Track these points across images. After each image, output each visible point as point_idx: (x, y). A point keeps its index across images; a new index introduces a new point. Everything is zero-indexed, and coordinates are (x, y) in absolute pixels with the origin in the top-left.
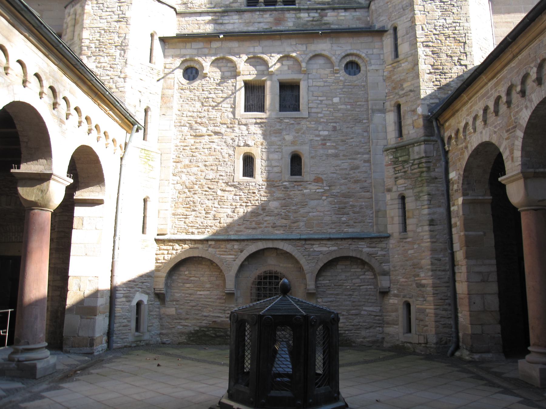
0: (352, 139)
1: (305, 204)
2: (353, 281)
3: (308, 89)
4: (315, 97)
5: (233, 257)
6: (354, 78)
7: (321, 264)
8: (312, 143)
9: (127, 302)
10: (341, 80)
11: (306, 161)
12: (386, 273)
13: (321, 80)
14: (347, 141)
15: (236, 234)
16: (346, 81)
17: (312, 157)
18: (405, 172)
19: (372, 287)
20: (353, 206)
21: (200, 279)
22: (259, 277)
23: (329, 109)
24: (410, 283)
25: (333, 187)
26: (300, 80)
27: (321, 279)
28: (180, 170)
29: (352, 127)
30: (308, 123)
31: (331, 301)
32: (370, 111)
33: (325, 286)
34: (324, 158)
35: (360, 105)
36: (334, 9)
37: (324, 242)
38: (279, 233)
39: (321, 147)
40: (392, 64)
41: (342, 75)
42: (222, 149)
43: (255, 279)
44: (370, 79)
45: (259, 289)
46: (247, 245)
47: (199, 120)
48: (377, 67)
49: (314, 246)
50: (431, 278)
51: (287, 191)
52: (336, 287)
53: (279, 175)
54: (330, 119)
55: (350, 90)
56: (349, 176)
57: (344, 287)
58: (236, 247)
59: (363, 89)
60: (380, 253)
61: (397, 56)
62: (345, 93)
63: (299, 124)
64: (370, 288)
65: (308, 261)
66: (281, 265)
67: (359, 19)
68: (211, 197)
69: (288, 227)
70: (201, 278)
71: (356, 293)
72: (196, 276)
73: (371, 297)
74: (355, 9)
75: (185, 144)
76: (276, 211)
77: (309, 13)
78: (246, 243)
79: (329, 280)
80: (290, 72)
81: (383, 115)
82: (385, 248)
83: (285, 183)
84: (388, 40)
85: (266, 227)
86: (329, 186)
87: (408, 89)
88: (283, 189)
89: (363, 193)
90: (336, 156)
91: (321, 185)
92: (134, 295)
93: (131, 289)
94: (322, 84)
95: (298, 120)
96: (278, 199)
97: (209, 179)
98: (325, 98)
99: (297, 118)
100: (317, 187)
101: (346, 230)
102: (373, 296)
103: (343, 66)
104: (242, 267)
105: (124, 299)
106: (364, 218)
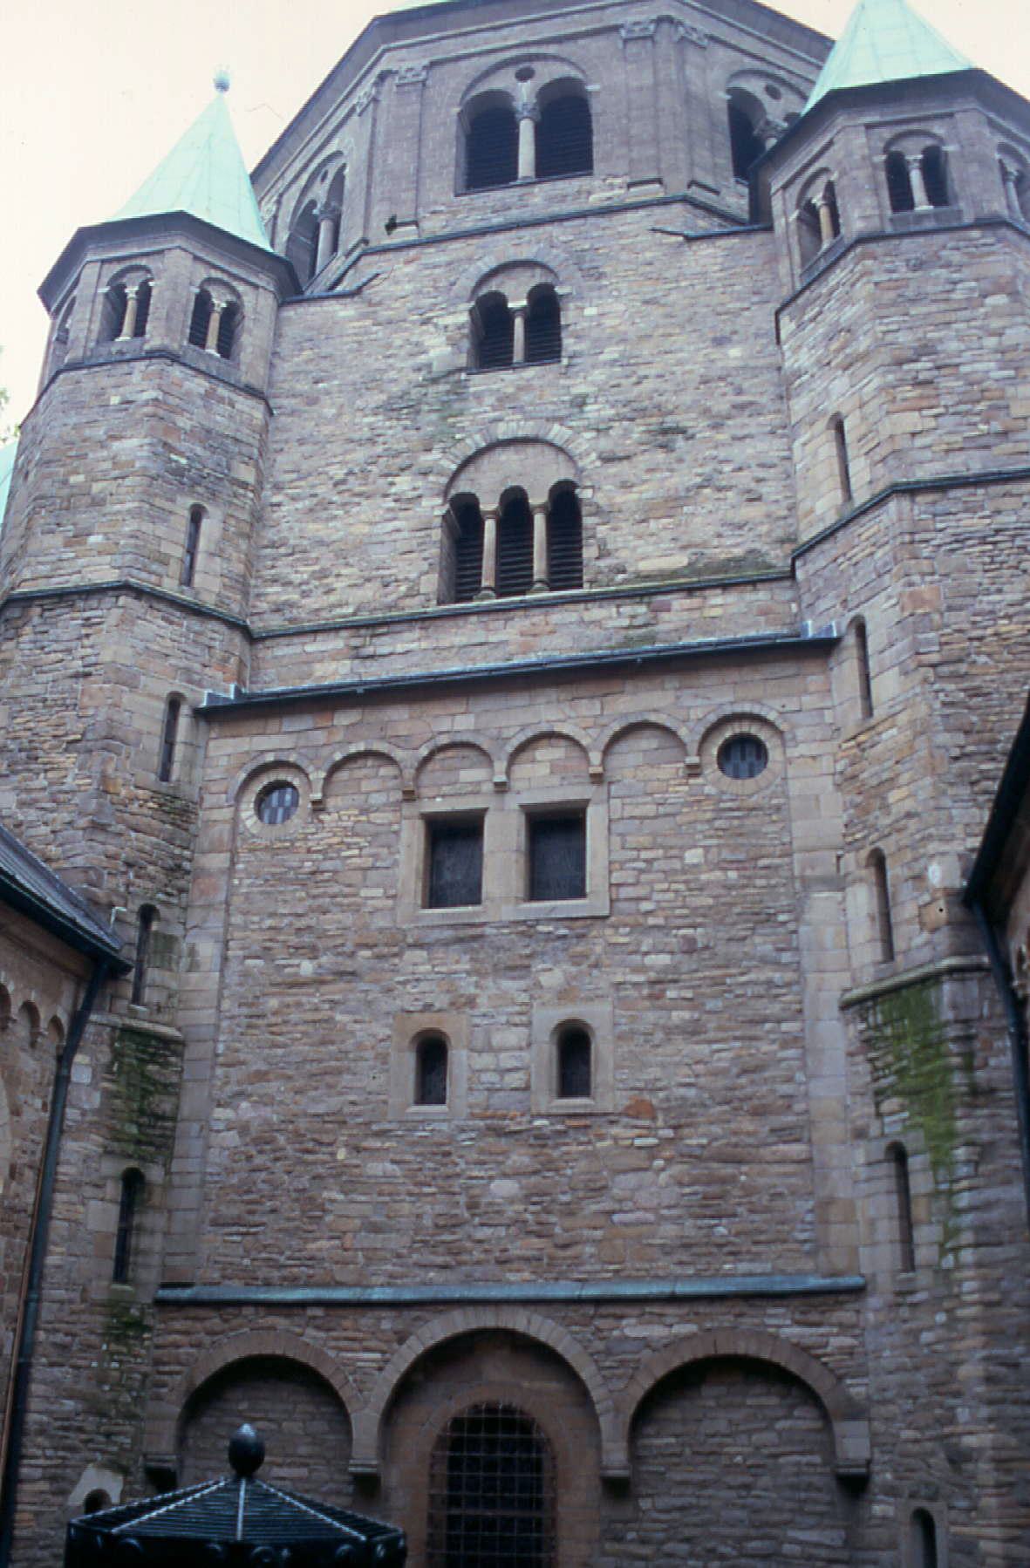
0: (742, 974)
1: (598, 1185)
2: (754, 1438)
5: (377, 1356)
6: (749, 785)
7: (646, 1383)
9: (54, 1493)
10: (708, 796)
11: (603, 1050)
12: (856, 1412)
14: (728, 981)
15: (389, 1285)
17: (620, 1037)
18: (901, 1073)
19: (817, 1459)
20: (749, 1191)
21: (280, 1425)
22: (457, 1423)
23: (674, 886)
24: (929, 1445)
25: (686, 1131)
26: (587, 802)
27: (650, 1430)
28: (236, 1088)
29: (744, 938)
30: (609, 931)
31: (682, 1509)
32: (798, 885)
33: (663, 1455)
34: (659, 1036)
35: (766, 868)
36: (690, 590)
37: (656, 1309)
38: (519, 1283)
39: (647, 1003)
40: (854, 738)
41: (713, 780)
42: (356, 1022)
43: (444, 1430)
44: (794, 788)
45: (454, 1464)
46: (417, 1319)
47: (294, 940)
48: (814, 749)
49: (624, 1322)
50: (991, 1426)
51: (544, 1146)
52: (699, 1459)
53: (519, 1095)
55: (736, 822)
56: (737, 1093)
57: (724, 1460)
58: (386, 1325)
59: (774, 817)
60: (835, 1342)
61: (869, 711)
63: (581, 937)
64: (808, 1464)
65: (605, 1372)
66: (526, 1384)
67: (764, 612)
68: (321, 1170)
69: (546, 1260)
70: (284, 1424)
71: (765, 1480)
72: (271, 1416)
73: (814, 1495)
74: (753, 583)
75: (254, 1011)
76: (511, 1211)
77: (618, 606)
78: (415, 1314)
79: (677, 1436)
80: (556, 780)
81: (839, 895)
82: (854, 1326)
83: (538, 1123)
84: (846, 668)
85: (478, 1263)
86: (676, 1128)
87: (897, 810)
88: (532, 1141)
89: (782, 1147)
90: (693, 1031)
91: (647, 1123)
92: (80, 1475)
93: (68, 1455)
94: (650, 810)
96: (516, 1174)
97: (317, 1115)
99: (577, 919)
100: (637, 1131)
101: (727, 1267)
102: (819, 1490)
103: (715, 751)
104: (405, 1391)
105: (44, 1486)
106: (786, 1227)
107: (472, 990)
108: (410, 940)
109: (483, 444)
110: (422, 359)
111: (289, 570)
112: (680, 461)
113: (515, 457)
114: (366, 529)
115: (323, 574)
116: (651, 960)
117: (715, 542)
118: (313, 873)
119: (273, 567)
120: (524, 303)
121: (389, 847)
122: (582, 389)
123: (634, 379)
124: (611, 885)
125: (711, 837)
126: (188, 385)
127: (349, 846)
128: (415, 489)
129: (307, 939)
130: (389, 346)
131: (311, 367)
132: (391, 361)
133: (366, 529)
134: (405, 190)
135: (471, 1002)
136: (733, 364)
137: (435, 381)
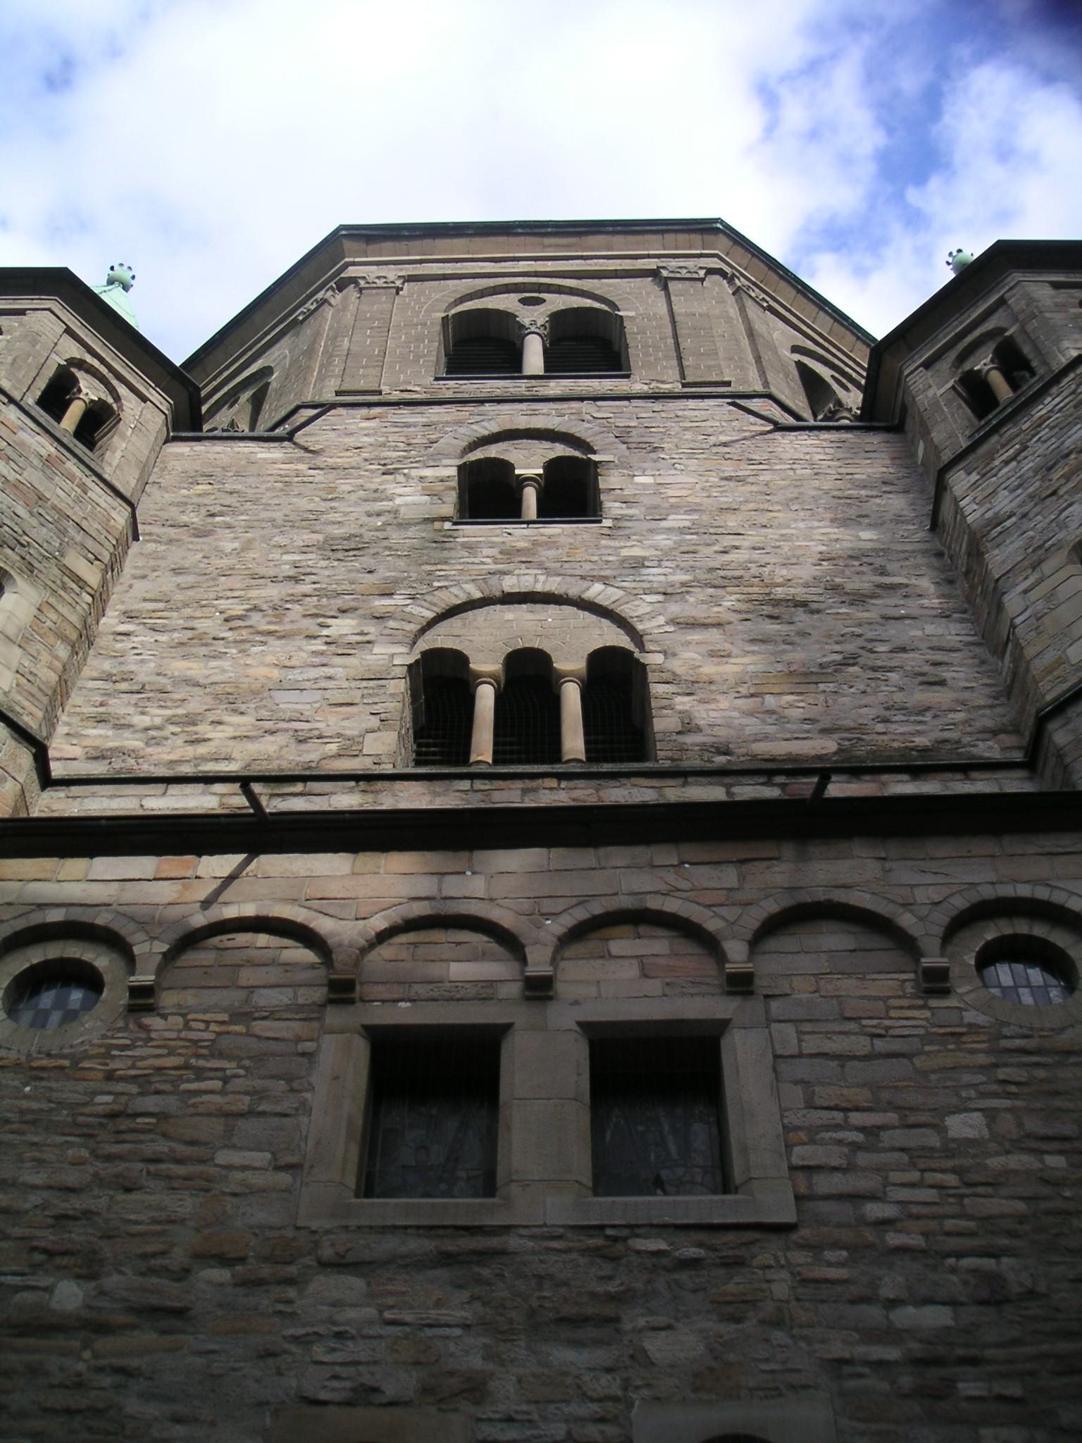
3: (774, 1069)
4: (824, 1114)
8: (850, 1384)
10: (970, 1025)
13: (852, 1026)
16: (1005, 1031)
23: (931, 1177)
30: (799, 1257)
42: (177, 1420)
47: (48, 1238)
54: (948, 1234)
55: (1041, 1073)
62: (1013, 1089)
63: (740, 1263)
77: (728, 787)
94: (861, 1045)
95: (730, 1237)
98: (892, 1117)
107: (476, 1362)
108: (327, 1253)
109: (478, 595)
110: (386, 505)
111: (131, 710)
112: (804, 634)
113: (530, 616)
114: (276, 674)
115: (191, 720)
116: (906, 1316)
117: (880, 727)
118: (113, 1115)
119: (102, 705)
120: (541, 471)
121: (289, 1078)
122: (637, 552)
123: (716, 548)
124: (793, 1169)
125: (995, 1095)
126: (23, 436)
127: (200, 1074)
128: (362, 634)
129: (78, 1235)
130: (334, 489)
131: (206, 500)
132: (334, 504)
133: (276, 674)
134: (366, 367)
135: (475, 1389)
136: (869, 545)
137: (404, 525)
